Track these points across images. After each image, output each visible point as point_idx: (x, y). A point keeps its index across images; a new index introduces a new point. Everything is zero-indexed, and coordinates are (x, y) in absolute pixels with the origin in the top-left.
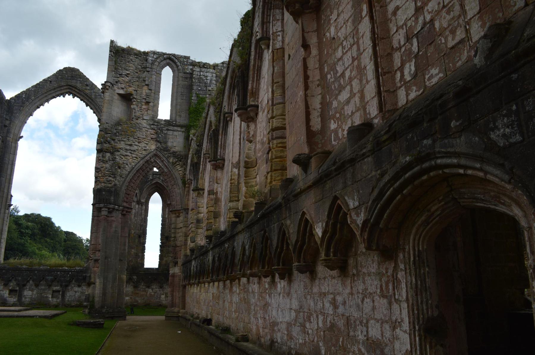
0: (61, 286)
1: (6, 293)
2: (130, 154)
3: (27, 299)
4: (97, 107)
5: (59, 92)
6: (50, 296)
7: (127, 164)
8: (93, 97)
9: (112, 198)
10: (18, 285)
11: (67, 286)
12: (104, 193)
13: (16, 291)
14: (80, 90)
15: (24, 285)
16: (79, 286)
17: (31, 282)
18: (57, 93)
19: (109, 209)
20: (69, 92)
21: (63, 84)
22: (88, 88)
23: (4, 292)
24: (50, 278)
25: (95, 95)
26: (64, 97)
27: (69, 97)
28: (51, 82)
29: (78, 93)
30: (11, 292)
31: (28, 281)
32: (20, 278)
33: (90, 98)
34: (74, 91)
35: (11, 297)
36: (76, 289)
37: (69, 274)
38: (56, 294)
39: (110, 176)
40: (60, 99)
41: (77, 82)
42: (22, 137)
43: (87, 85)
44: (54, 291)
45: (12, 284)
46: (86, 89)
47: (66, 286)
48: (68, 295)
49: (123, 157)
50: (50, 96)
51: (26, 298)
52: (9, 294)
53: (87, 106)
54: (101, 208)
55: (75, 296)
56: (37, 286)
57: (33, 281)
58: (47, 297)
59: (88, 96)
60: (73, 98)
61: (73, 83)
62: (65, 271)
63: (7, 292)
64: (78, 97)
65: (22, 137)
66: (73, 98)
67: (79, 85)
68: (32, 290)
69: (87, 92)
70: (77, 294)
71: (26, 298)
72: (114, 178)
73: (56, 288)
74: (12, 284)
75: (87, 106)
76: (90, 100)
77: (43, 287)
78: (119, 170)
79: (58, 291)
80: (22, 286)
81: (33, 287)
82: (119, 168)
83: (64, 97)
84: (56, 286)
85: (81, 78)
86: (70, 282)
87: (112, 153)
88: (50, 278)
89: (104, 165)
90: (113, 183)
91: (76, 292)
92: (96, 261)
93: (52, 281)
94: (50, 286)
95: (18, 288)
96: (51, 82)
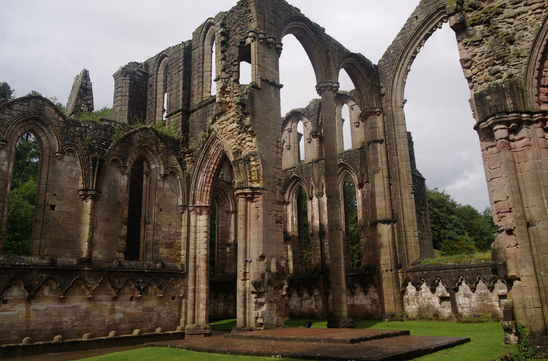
2: (525, 9)
3: (465, 309)
7: (525, 29)
9: (509, 101)
12: (488, 98)
15: (457, 290)
19: (508, 123)
31: (460, 284)
39: (495, 64)
45: (441, 289)
49: (512, 20)
51: (463, 308)
54: (490, 128)
65: (406, 101)
71: (463, 308)
72: (503, 64)
78: (512, 47)
81: (469, 292)
82: (511, 42)
87: (487, 23)
89: (476, 50)
90: (505, 75)
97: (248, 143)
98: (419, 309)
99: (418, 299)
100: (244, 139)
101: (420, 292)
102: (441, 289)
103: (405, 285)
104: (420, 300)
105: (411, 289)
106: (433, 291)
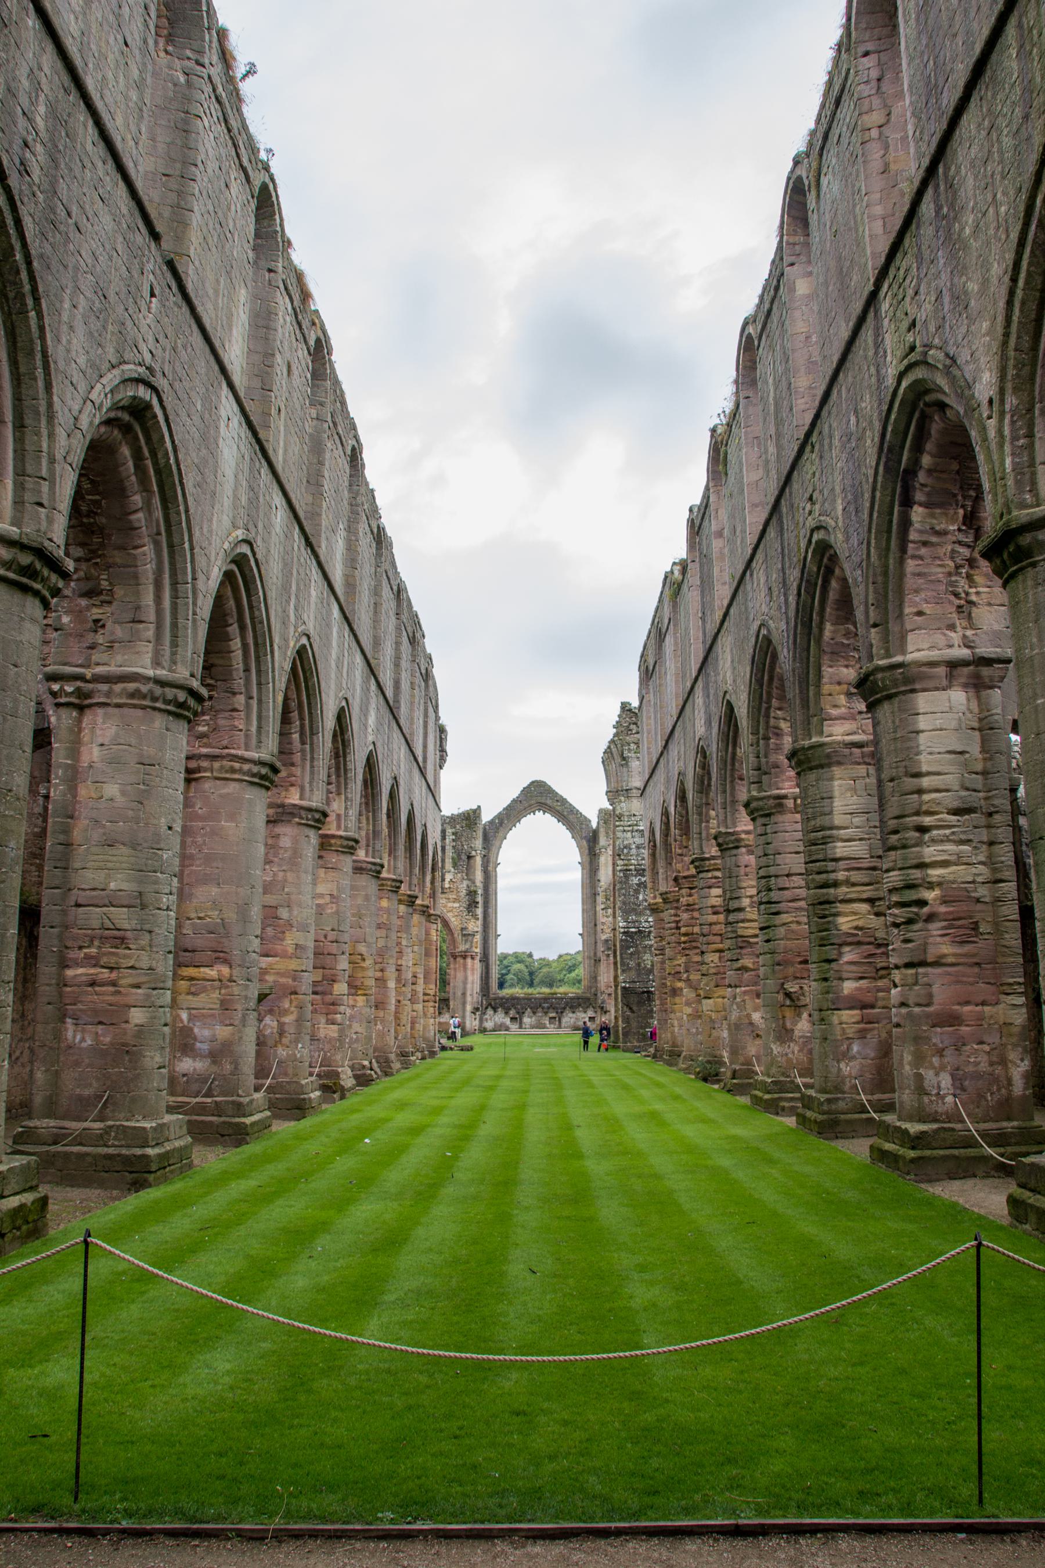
1: (507, 1021)
10: (518, 1013)
24: (546, 1005)
27: (539, 814)
30: (513, 1019)
36: (571, 1015)
45: (512, 1013)
47: (561, 1013)
56: (534, 1013)
67: (549, 802)
68: (531, 1017)
69: (558, 808)
70: (572, 1020)
80: (521, 1014)
86: (564, 1008)
88: (546, 1005)
92: (610, 995)
93: (548, 1008)
94: (546, 1013)
105: (490, 1012)
106: (506, 1013)
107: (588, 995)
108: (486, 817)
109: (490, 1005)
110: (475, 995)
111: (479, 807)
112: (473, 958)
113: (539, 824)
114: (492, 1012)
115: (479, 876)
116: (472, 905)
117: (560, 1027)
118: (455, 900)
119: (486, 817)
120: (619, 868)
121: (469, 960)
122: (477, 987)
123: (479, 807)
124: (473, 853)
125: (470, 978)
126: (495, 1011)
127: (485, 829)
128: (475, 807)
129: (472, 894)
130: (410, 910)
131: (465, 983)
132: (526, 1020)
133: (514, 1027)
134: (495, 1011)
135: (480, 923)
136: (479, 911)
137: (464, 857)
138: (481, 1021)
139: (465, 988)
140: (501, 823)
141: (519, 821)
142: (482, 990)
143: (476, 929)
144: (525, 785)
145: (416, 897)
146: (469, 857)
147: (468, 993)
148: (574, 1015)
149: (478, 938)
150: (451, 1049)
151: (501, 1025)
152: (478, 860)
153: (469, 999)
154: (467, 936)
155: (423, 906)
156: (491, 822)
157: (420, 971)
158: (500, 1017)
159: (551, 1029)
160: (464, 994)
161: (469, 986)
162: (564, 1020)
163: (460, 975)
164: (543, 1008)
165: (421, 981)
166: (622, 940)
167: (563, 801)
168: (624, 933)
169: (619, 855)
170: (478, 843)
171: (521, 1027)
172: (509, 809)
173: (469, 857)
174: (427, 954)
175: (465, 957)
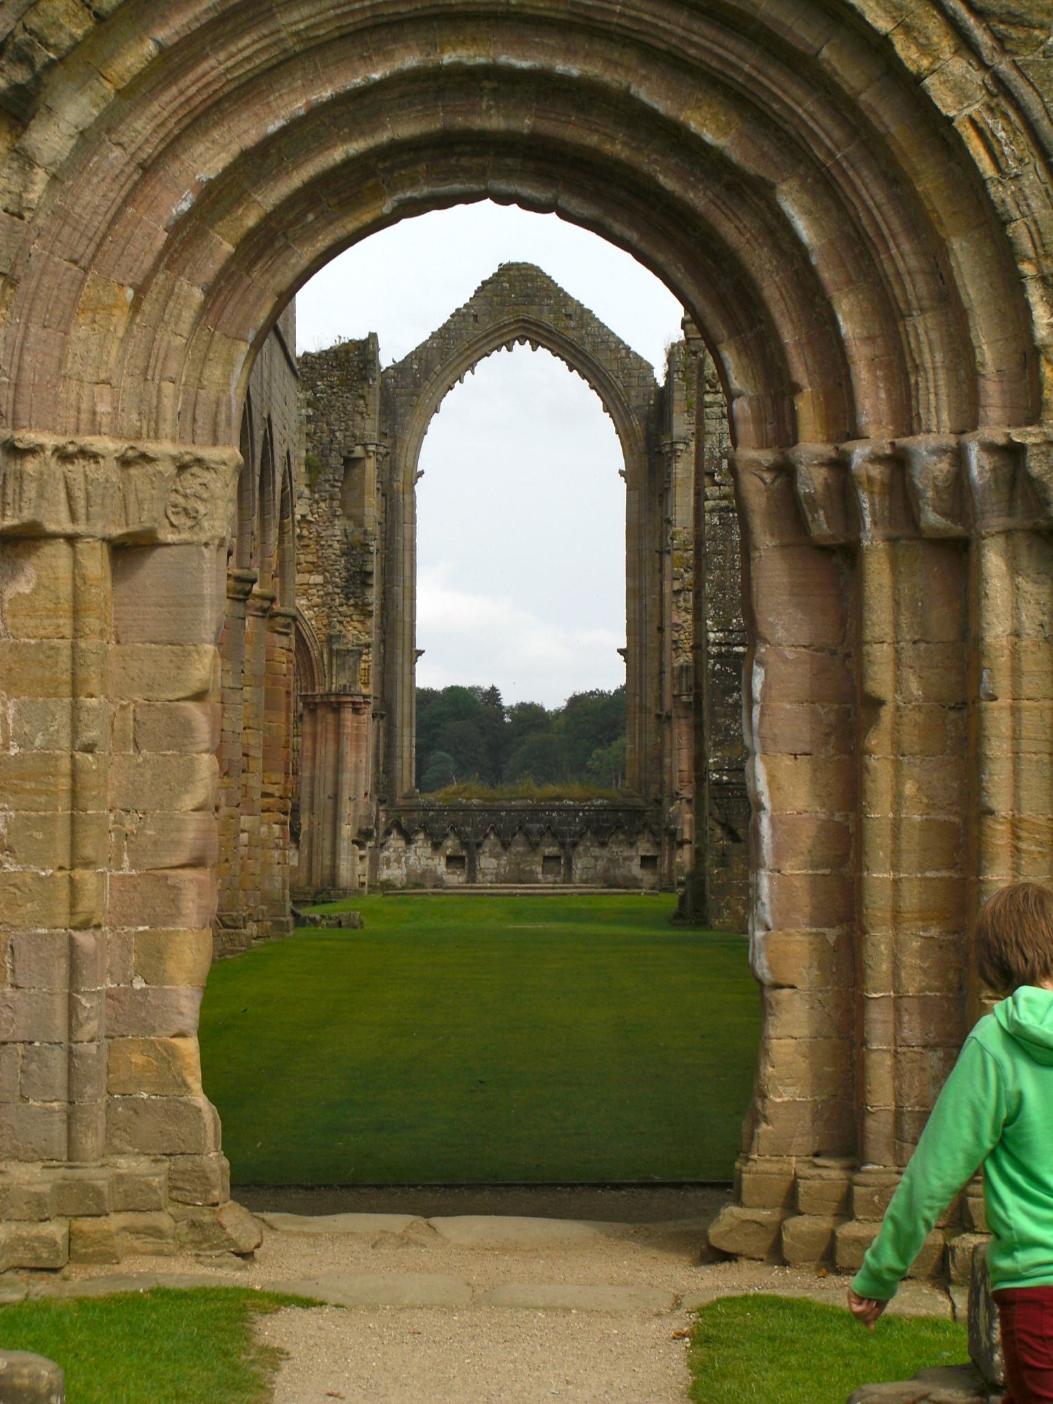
0: (562, 845)
1: (440, 864)
4: (600, 376)
5: (498, 342)
6: (539, 869)
8: (588, 348)
10: (465, 845)
11: (574, 845)
13: (462, 858)
14: (551, 332)
15: (479, 845)
16: (603, 845)
17: (492, 837)
18: (493, 344)
20: (522, 336)
21: (506, 319)
22: (573, 324)
23: (436, 861)
25: (594, 344)
26: (510, 350)
27: (522, 350)
28: (475, 316)
29: (547, 338)
30: (450, 860)
31: (486, 836)
32: (469, 829)
33: (580, 352)
34: (536, 333)
35: (454, 873)
36: (596, 851)
37: (577, 815)
38: (551, 864)
40: (499, 357)
41: (541, 311)
42: (422, 473)
43: (569, 316)
44: (547, 859)
45: (451, 845)
46: (567, 328)
47: (569, 846)
48: (579, 866)
50: (476, 356)
51: (485, 875)
52: (447, 865)
53: (571, 370)
55: (595, 867)
56: (506, 846)
57: (497, 835)
58: (532, 872)
59: (573, 346)
60: (534, 350)
61: (533, 313)
62: (568, 810)
63: (443, 861)
64: (544, 346)
65: (422, 473)
66: (534, 350)
67: (547, 319)
68: (497, 857)
69: (572, 335)
70: (601, 864)
71: (485, 875)
73: (551, 849)
74: (449, 843)
75: (571, 370)
76: (581, 357)
77: (521, 849)
79: (557, 858)
81: (498, 849)
83: (510, 350)
84: (549, 846)
85: (550, 298)
86: (582, 835)
91: (596, 858)
94: (534, 847)
95: (464, 853)
96: (475, 316)
97: (356, 624)
98: (408, 875)
99: (408, 859)
100: (350, 616)
101: (413, 846)
102: (451, 845)
103: (388, 833)
104: (412, 861)
105: (395, 841)
106: (436, 846)
107: (639, 801)
108: (388, 356)
109: (397, 825)
110: (362, 800)
111: (373, 337)
112: (356, 711)
113: (524, 376)
114: (402, 843)
115: (372, 508)
116: (358, 579)
117: (568, 879)
118: (314, 568)
119: (388, 356)
120: (709, 504)
121: (348, 715)
122: (365, 781)
123: (373, 337)
124: (359, 451)
125: (350, 759)
126: (409, 841)
127: (384, 387)
128: (364, 336)
129: (355, 550)
130: (240, 608)
131: (338, 769)
132: (486, 862)
133: (455, 878)
134: (409, 841)
135: (372, 623)
136: (373, 596)
137: (335, 460)
138: (375, 865)
139: (337, 784)
140: (426, 371)
141: (471, 367)
142: (376, 784)
143: (365, 639)
144: (487, 276)
145: (253, 582)
146: (350, 462)
147: (346, 794)
148: (605, 852)
149: (370, 659)
150: (313, 921)
151: (424, 874)
152: (371, 465)
153: (347, 809)
154: (345, 656)
155: (262, 597)
156: (401, 368)
157: (255, 740)
158: (421, 857)
159: (545, 883)
160: (336, 798)
161: (347, 777)
162: (579, 865)
163: (326, 751)
164: (527, 834)
165: (257, 765)
166: (714, 674)
167: (584, 316)
168: (719, 656)
169: (711, 475)
170: (370, 427)
171: (472, 878)
172: (444, 335)
173: (350, 462)
174: (270, 705)
175: (337, 708)
